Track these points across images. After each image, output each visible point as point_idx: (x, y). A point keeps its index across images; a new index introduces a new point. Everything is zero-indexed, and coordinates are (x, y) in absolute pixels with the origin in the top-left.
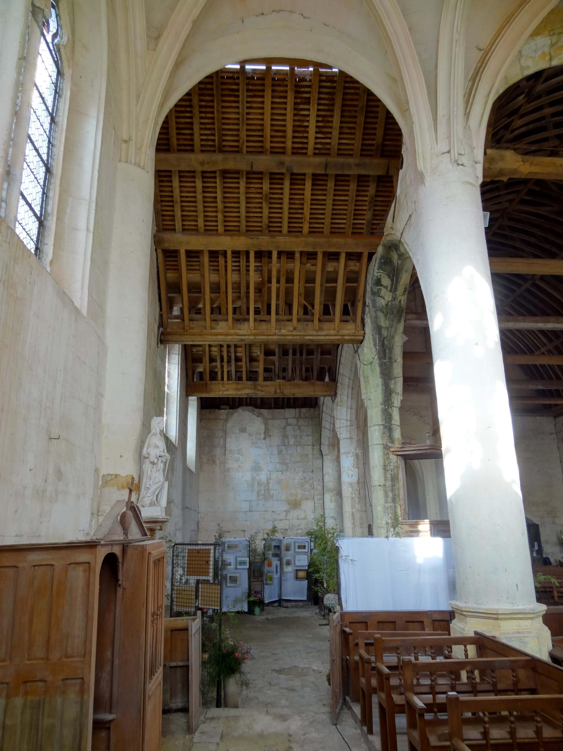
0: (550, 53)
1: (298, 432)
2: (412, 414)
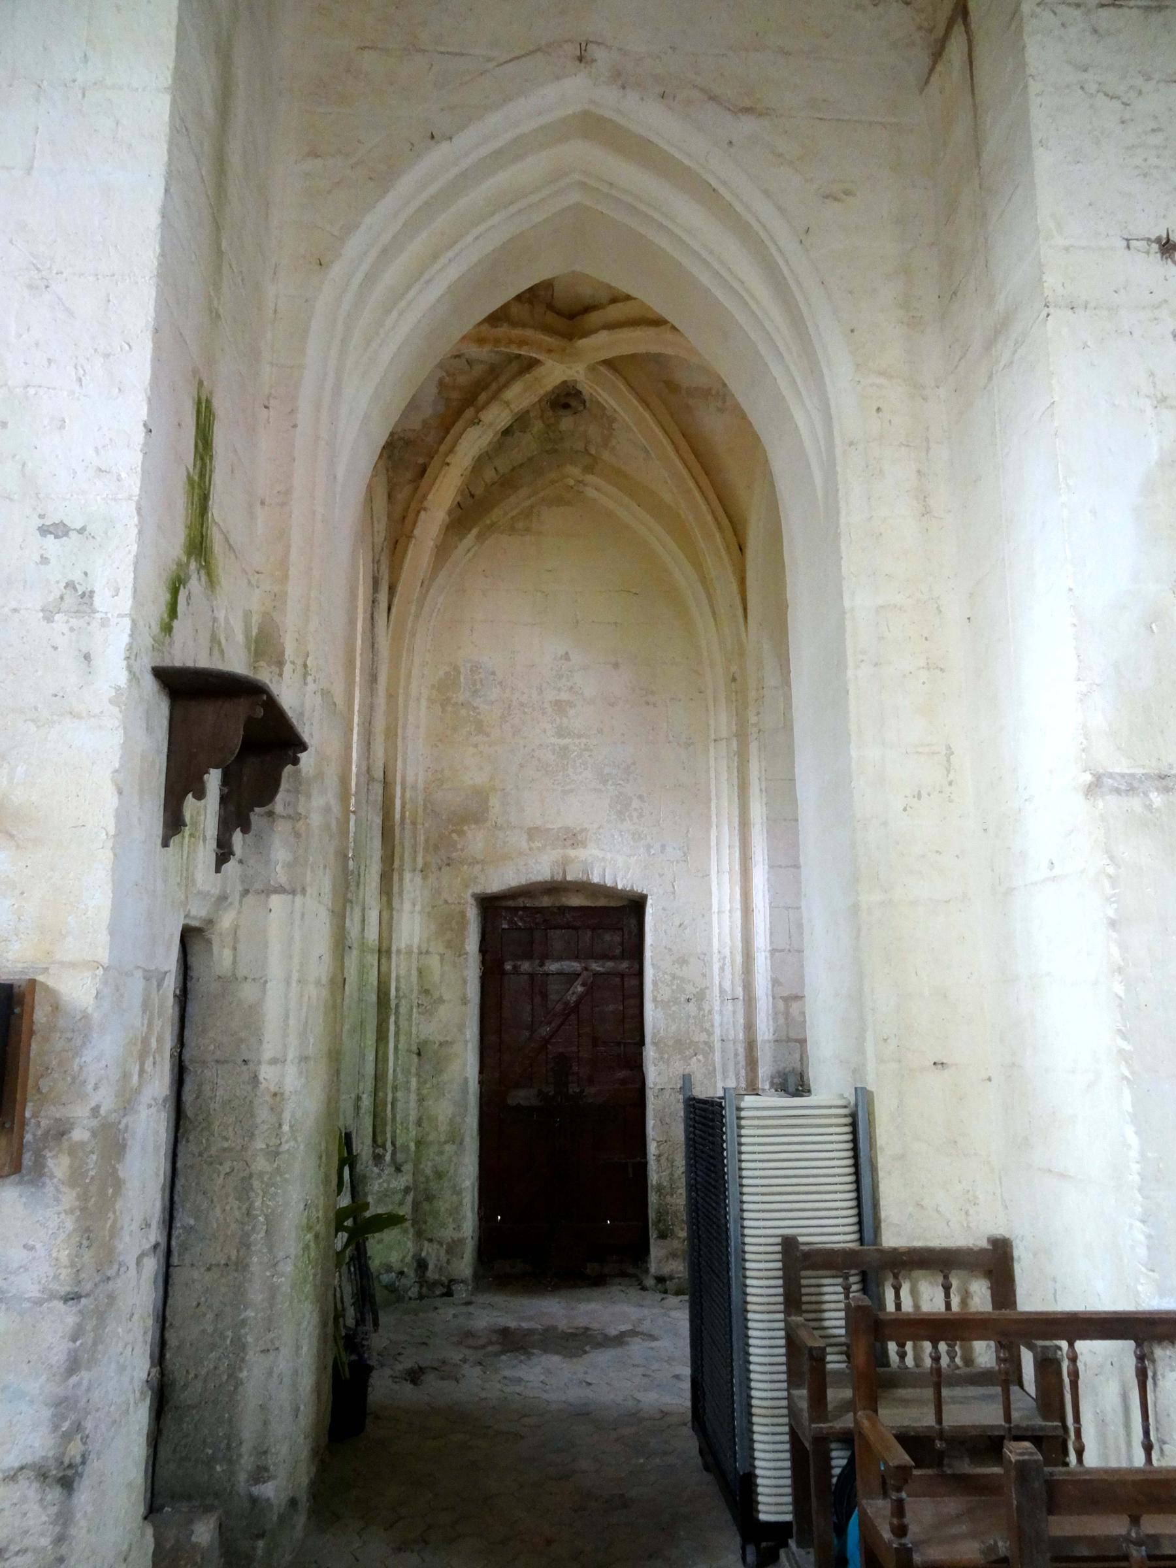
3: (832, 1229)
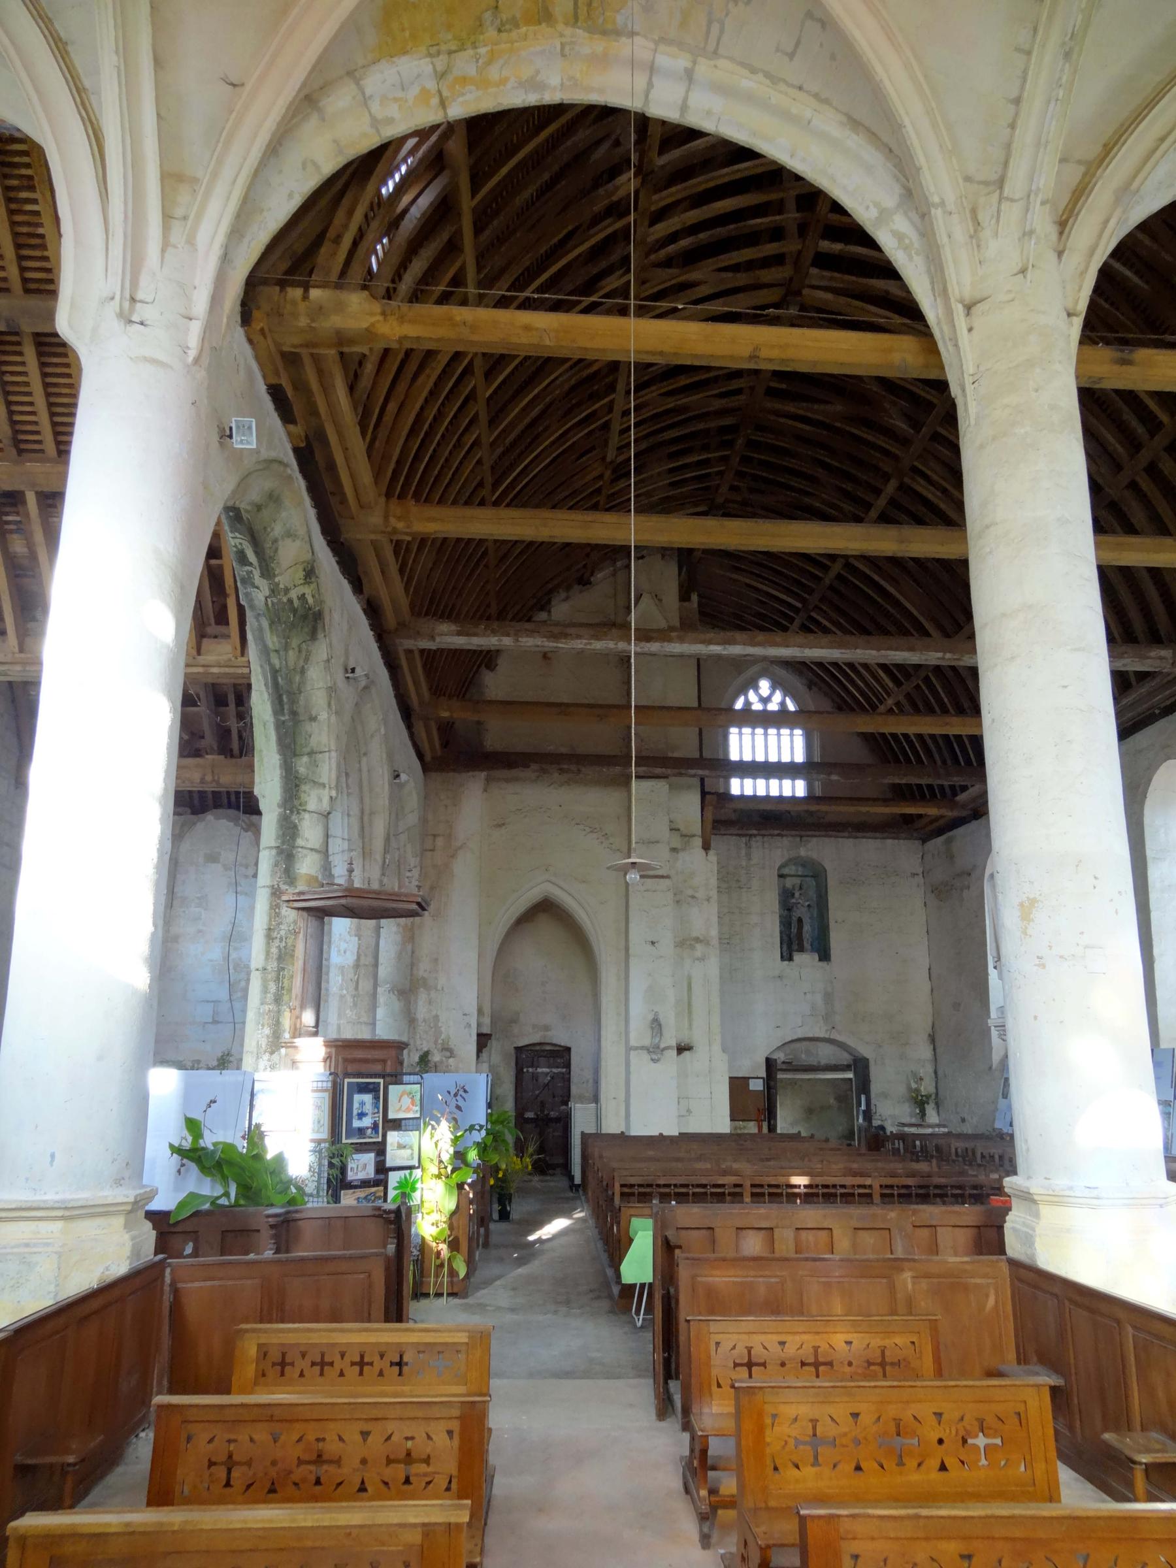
0: (439, 92)
2: (588, 829)
3: (591, 1129)
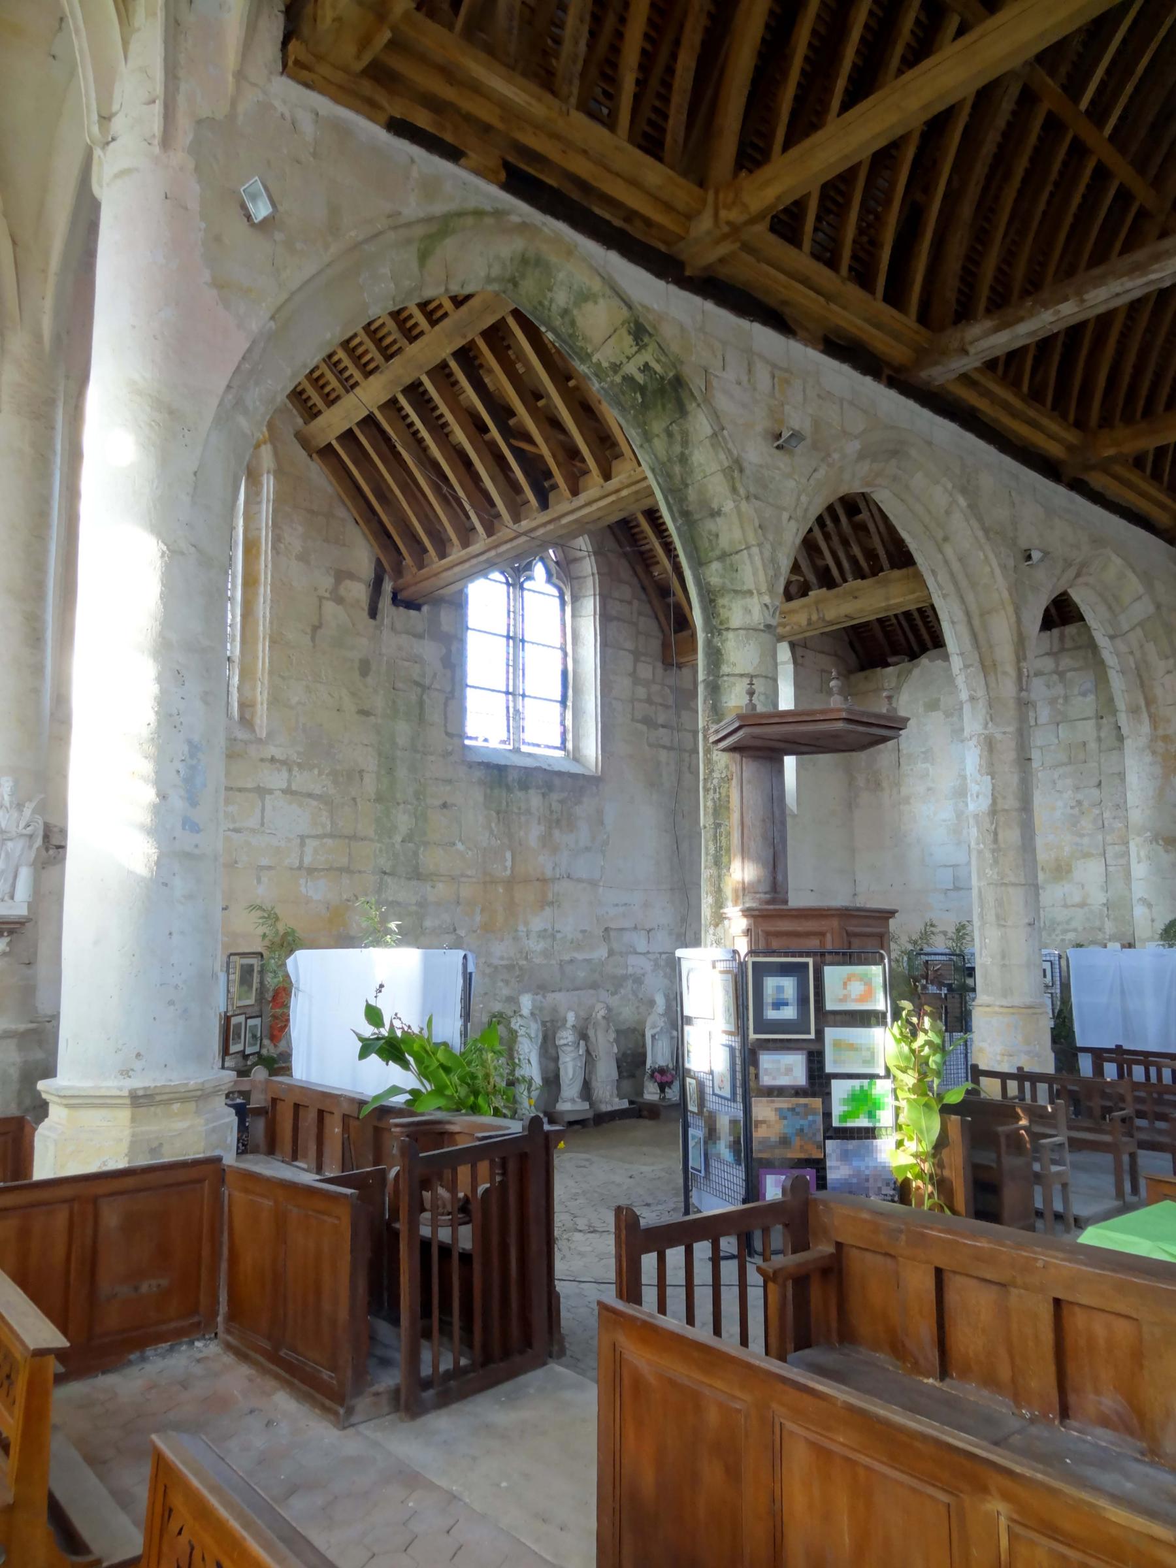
1: (1059, 690)
